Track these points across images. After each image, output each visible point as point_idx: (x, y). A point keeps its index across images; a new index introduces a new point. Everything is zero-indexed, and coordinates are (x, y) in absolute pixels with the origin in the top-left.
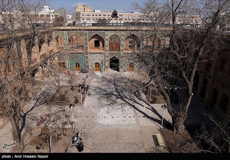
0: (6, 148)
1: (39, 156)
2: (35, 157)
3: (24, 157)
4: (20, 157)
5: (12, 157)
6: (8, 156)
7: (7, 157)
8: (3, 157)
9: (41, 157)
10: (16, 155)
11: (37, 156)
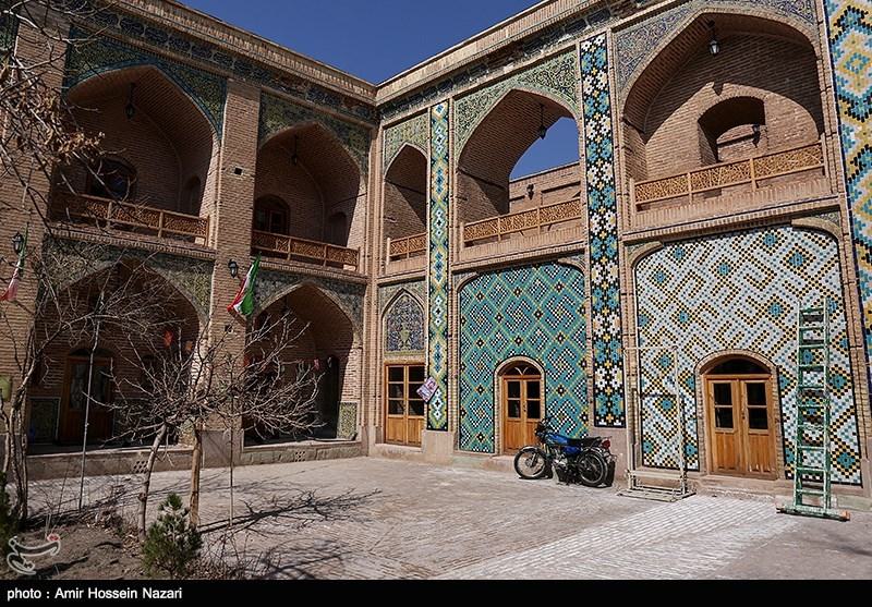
0: (20, 561)
1: (148, 593)
2: (131, 594)
3: (93, 596)
4: (77, 594)
5: (44, 595)
6: (32, 591)
7: (26, 594)
8: (12, 595)
9: (156, 595)
10: (60, 589)
11: (140, 593)
